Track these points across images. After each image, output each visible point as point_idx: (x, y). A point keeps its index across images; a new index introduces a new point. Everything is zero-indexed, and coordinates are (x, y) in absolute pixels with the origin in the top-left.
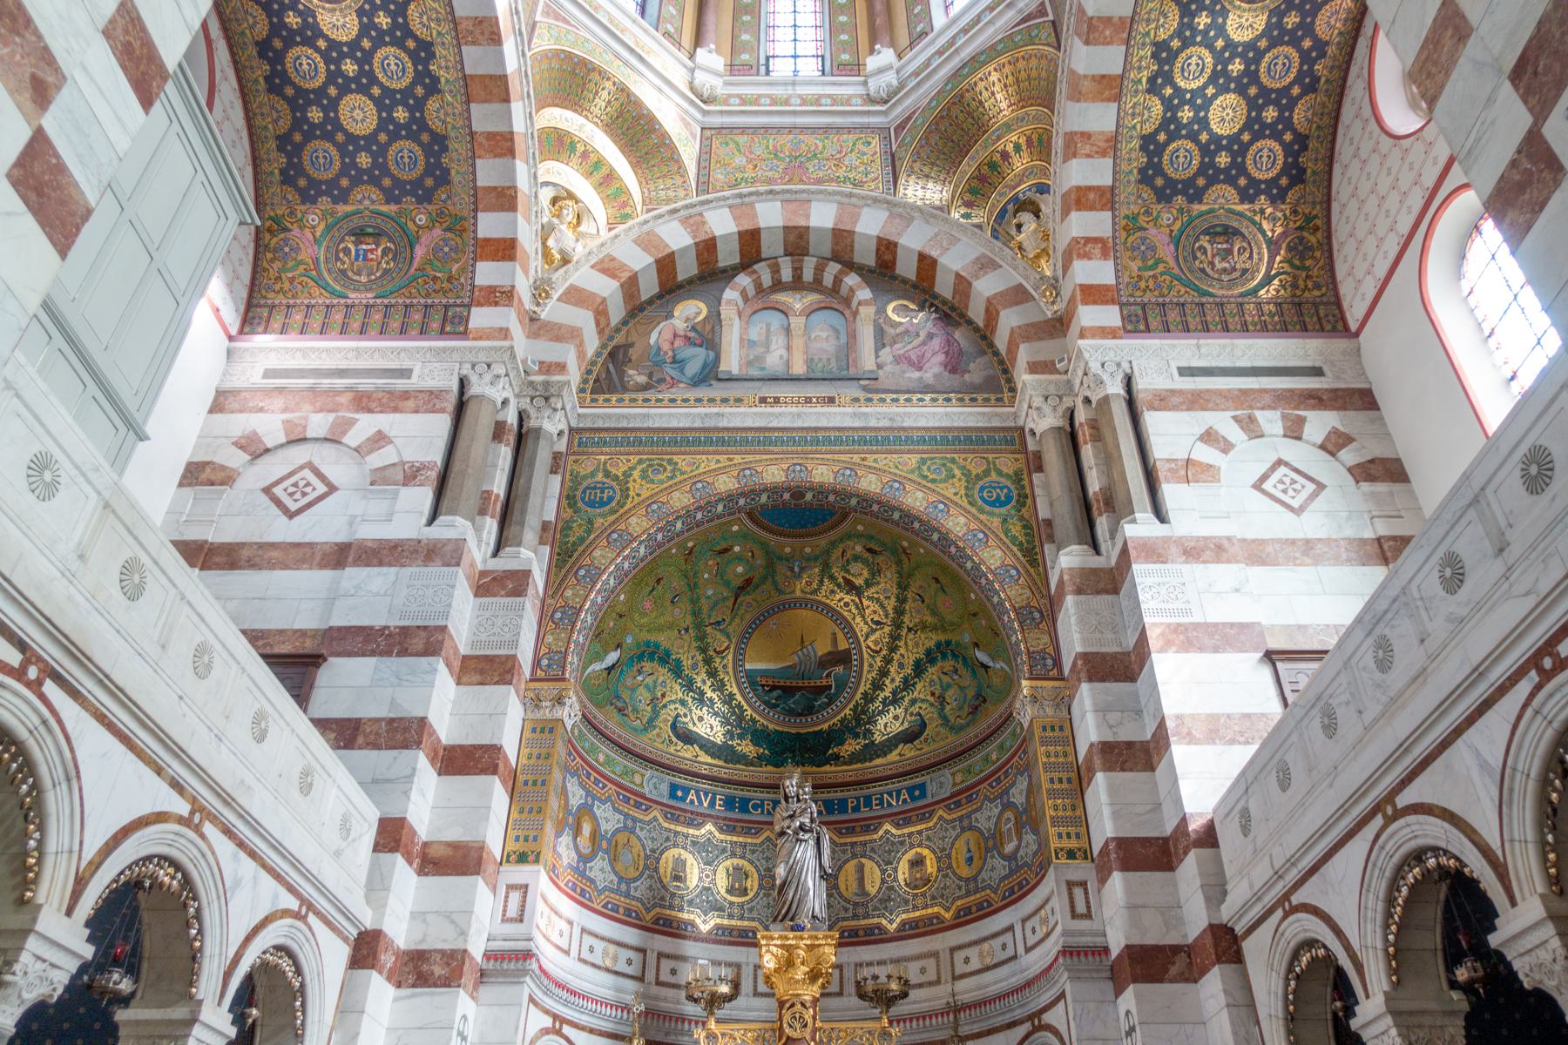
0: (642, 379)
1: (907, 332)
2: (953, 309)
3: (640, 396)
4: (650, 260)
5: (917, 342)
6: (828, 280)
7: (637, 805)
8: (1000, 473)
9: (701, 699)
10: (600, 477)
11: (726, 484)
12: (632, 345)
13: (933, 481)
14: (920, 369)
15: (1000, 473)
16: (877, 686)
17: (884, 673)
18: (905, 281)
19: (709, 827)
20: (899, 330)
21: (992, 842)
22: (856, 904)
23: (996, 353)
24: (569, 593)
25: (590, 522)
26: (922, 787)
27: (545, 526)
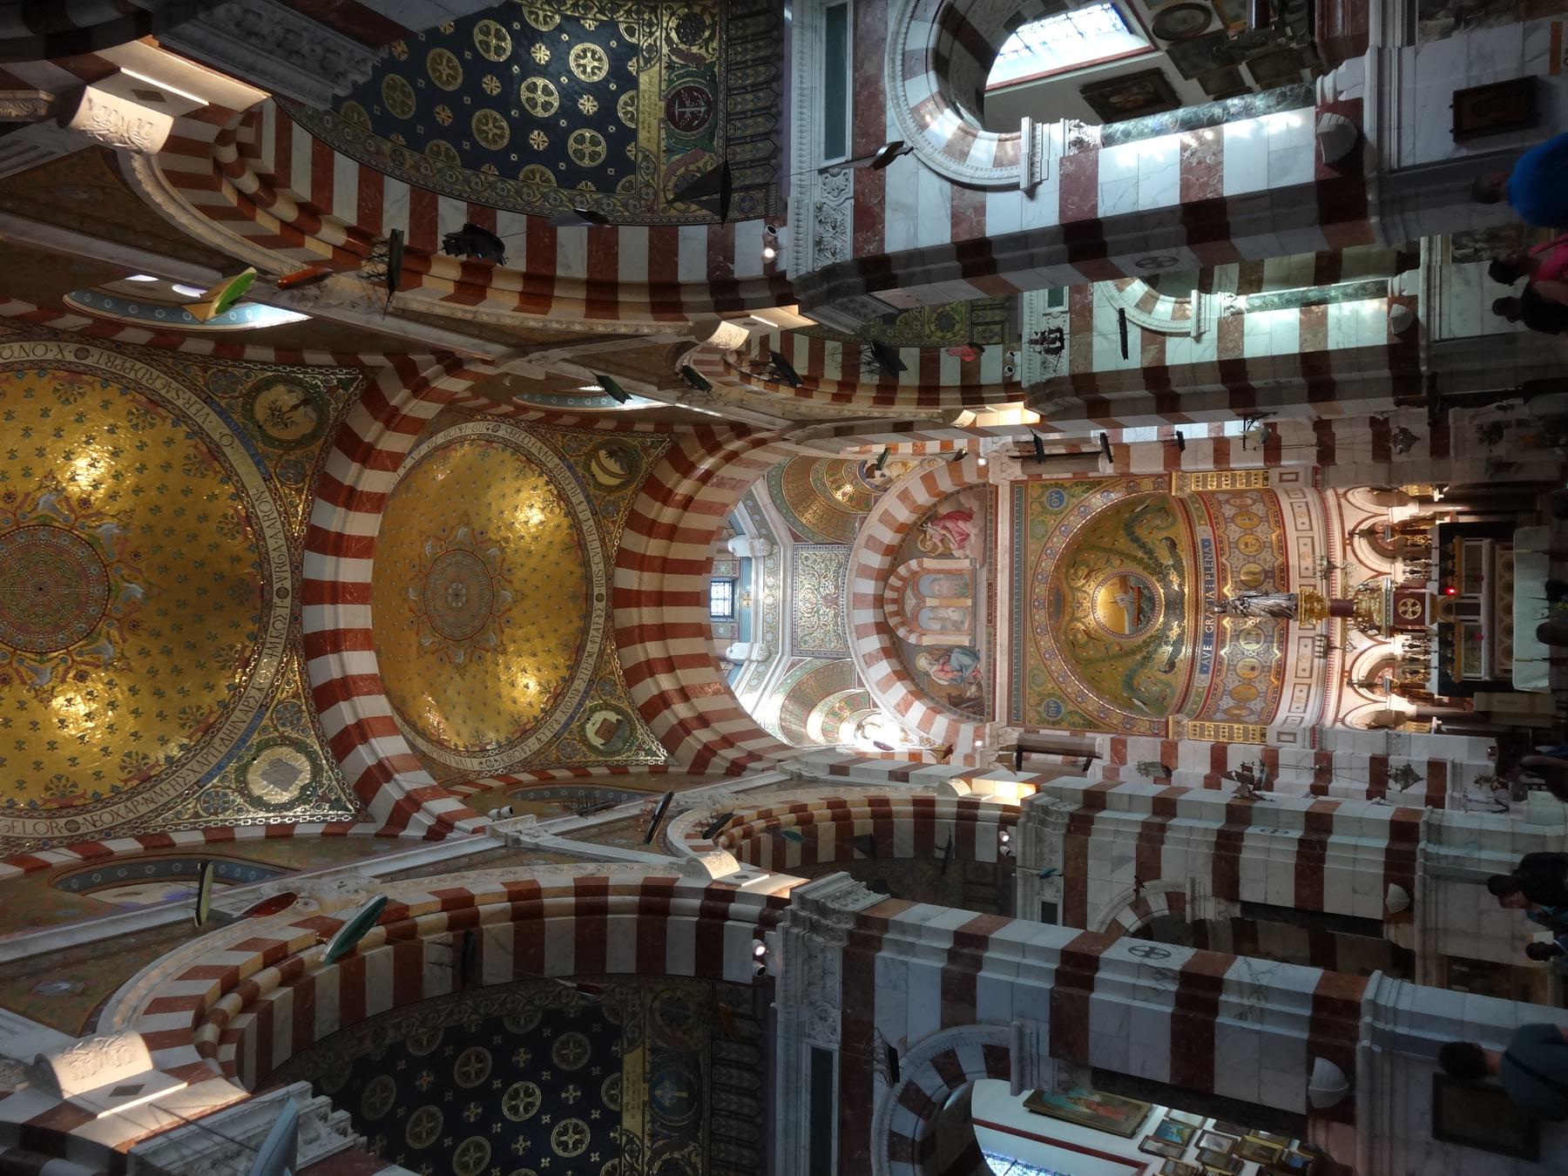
0: (974, 688)
1: (942, 541)
2: (924, 514)
3: (985, 689)
4: (899, 684)
5: (948, 535)
6: (899, 584)
7: (1216, 689)
8: (1040, 496)
9: (1148, 659)
10: (1041, 709)
11: (1047, 642)
12: (949, 695)
13: (1046, 532)
14: (968, 535)
15: (1040, 496)
16: (1140, 561)
17: (1135, 559)
18: (903, 540)
19: (1222, 652)
20: (940, 544)
21: (1244, 511)
22: (1266, 577)
23: (958, 492)
24: (1114, 722)
25: (1070, 712)
26: (1203, 541)
27: (1074, 734)
